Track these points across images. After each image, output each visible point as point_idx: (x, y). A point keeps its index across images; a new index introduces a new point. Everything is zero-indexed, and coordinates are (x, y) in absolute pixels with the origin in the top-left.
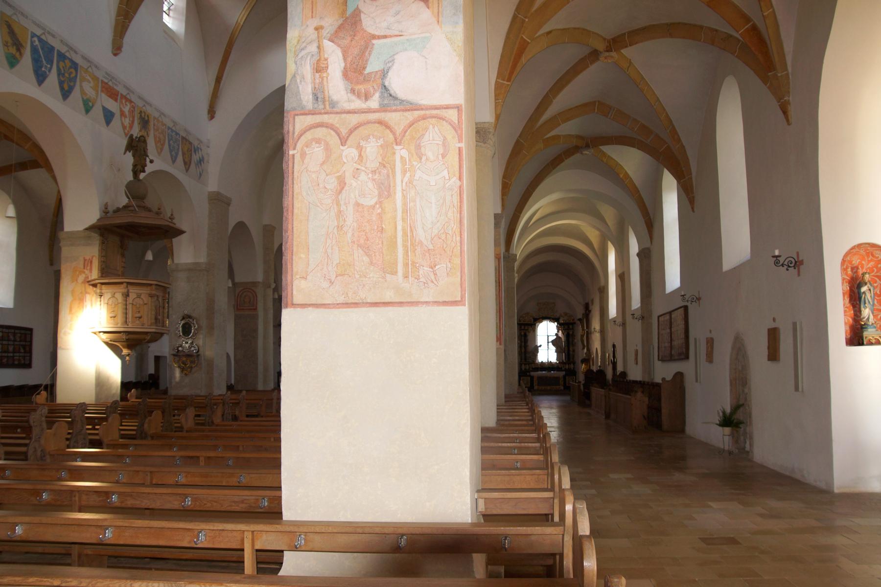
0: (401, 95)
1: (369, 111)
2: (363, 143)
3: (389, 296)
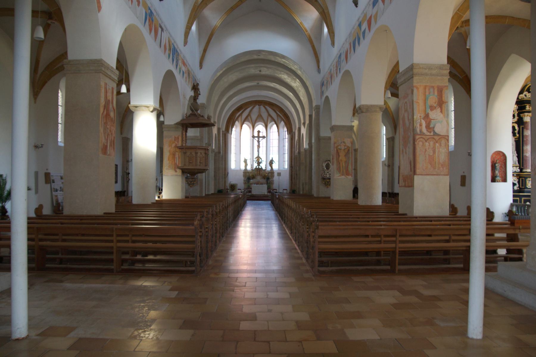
0: (437, 133)
1: (431, 135)
2: (430, 142)
3: (435, 173)
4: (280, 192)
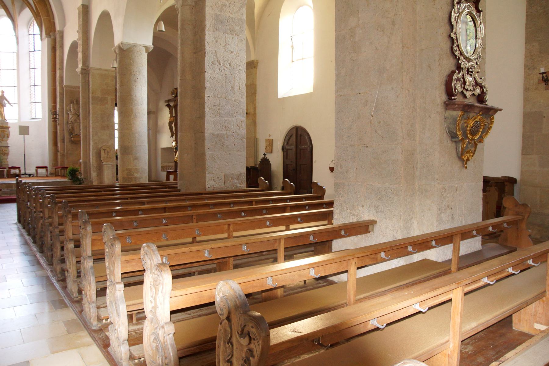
4: (27, 172)
